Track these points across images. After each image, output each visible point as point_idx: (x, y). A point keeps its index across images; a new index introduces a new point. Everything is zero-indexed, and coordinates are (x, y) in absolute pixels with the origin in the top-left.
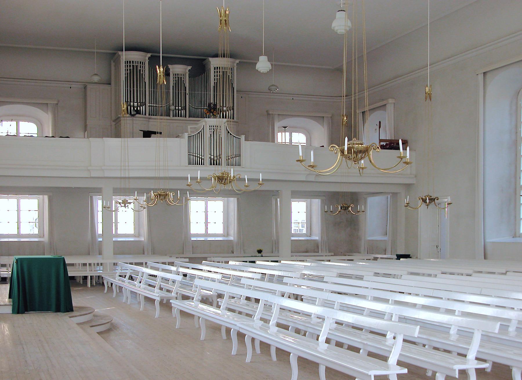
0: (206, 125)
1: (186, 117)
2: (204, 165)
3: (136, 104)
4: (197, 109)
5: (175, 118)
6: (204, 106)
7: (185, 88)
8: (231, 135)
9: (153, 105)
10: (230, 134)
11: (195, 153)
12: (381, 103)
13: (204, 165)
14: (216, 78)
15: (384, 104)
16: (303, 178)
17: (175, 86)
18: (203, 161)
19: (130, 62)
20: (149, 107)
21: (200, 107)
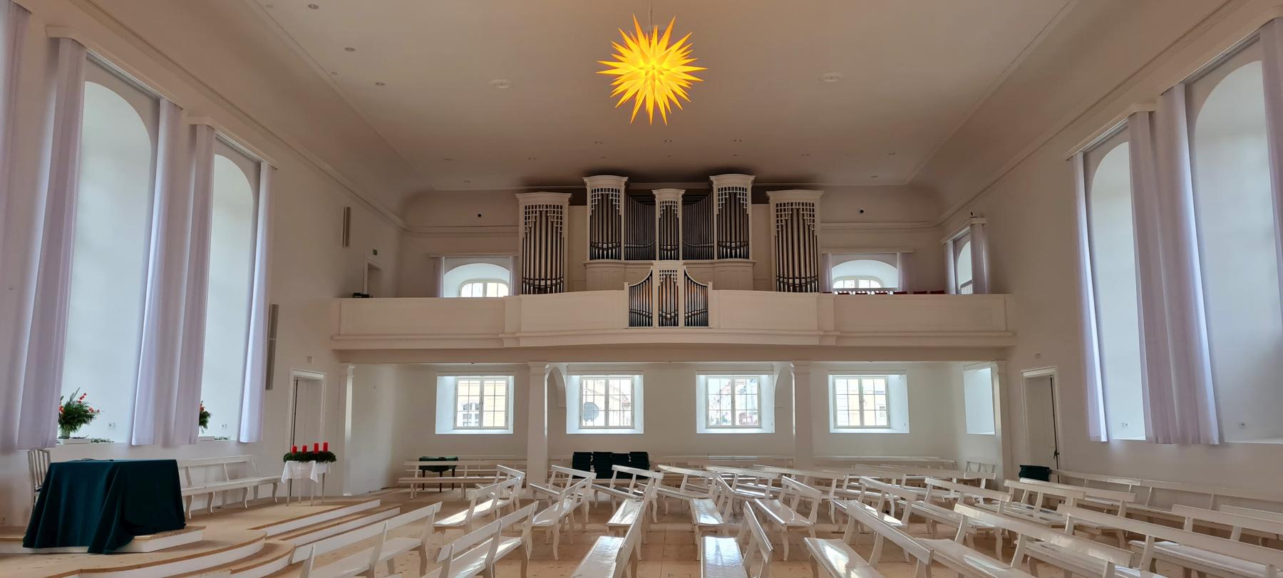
7: (678, 219)
8: (689, 281)
10: (692, 281)
19: (598, 190)
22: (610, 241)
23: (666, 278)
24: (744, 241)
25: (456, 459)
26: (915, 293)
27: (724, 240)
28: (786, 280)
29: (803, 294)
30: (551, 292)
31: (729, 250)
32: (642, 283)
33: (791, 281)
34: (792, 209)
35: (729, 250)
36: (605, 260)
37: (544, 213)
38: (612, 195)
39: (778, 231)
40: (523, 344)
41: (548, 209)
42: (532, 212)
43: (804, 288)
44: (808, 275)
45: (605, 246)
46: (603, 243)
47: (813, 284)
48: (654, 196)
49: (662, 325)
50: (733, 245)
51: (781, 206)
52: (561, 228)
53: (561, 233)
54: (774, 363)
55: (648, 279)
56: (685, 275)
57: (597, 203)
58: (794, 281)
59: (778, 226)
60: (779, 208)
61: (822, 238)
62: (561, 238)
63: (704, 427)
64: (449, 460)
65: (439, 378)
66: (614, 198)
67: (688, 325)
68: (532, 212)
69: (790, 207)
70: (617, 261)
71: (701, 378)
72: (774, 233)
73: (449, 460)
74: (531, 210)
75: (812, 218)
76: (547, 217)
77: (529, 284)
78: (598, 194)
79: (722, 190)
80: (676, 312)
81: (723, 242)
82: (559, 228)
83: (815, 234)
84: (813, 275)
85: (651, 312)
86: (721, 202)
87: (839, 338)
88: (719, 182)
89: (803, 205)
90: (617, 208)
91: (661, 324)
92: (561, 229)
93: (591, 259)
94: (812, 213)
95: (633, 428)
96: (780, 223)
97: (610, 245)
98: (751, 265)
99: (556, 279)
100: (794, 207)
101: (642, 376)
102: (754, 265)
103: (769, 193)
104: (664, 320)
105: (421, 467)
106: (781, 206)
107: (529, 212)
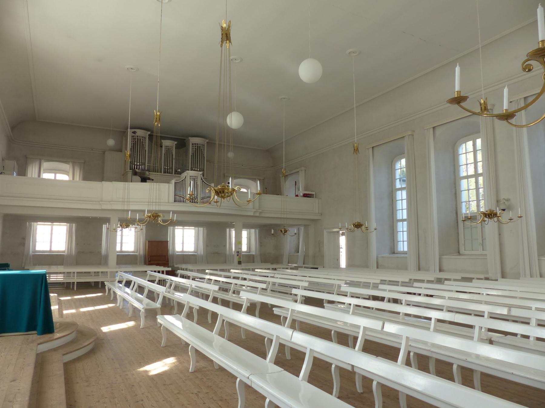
0: (187, 175)
1: (172, 174)
2: (185, 202)
3: (138, 164)
5: (165, 174)
7: (173, 155)
12: (297, 170)
13: (185, 202)
14: (193, 150)
15: (298, 171)
16: (252, 214)
24: (201, 169)
46: (137, 162)
56: (202, 179)
87: (260, 213)
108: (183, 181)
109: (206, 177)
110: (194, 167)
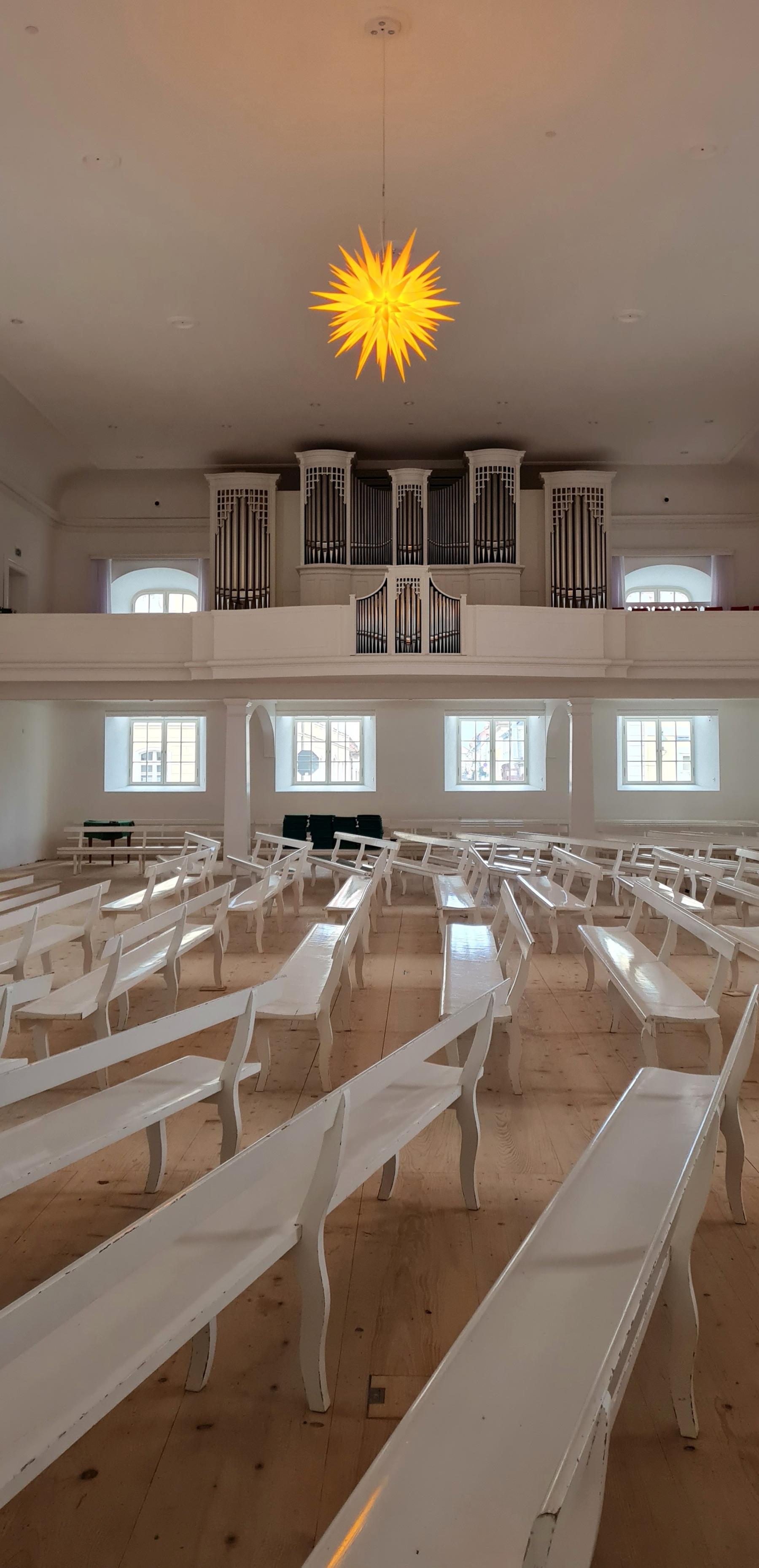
4: (445, 547)
6: (457, 541)
7: (422, 509)
9: (359, 545)
10: (439, 593)
11: (369, 630)
17: (401, 508)
18: (384, 645)
20: (353, 550)
21: (492, 541)
22: (331, 538)
23: (405, 589)
24: (509, 540)
25: (131, 824)
26: (733, 609)
27: (483, 538)
28: (563, 592)
29: (587, 610)
30: (254, 607)
31: (489, 552)
32: (374, 595)
33: (570, 593)
34: (574, 496)
35: (489, 552)
36: (325, 565)
37: (243, 502)
38: (334, 476)
39: (555, 527)
40: (218, 674)
41: (249, 496)
42: (228, 498)
43: (587, 602)
44: (593, 585)
45: (325, 545)
46: (322, 542)
47: (600, 597)
48: (390, 479)
49: (400, 651)
50: (495, 544)
51: (559, 492)
52: (266, 521)
53: (266, 528)
54: (547, 701)
55: (382, 590)
56: (431, 584)
57: (313, 487)
58: (574, 593)
59: (555, 519)
60: (557, 495)
61: (613, 535)
62: (266, 534)
63: (455, 782)
64: (123, 825)
65: (107, 719)
66: (337, 481)
67: (434, 651)
68: (228, 498)
69: (571, 494)
70: (340, 565)
71: (452, 721)
72: (549, 529)
73: (123, 825)
74: (225, 496)
75: (600, 509)
76: (247, 506)
77: (225, 596)
78: (315, 476)
79: (481, 471)
80: (418, 634)
81: (481, 540)
82: (263, 522)
83: (603, 531)
84: (599, 585)
85: (385, 634)
86: (479, 487)
87: (631, 668)
88: (478, 459)
89: (588, 492)
90: (341, 495)
91: (399, 650)
92: (266, 523)
93: (306, 563)
94: (600, 502)
95: (363, 784)
96: (557, 516)
97: (331, 544)
98: (519, 572)
99: (260, 589)
100: (576, 494)
101: (374, 717)
102: (522, 572)
103: (544, 475)
104: (402, 645)
105: (86, 834)
106: (559, 492)
107: (223, 498)
108: (380, 593)
109: (521, 564)
110: (489, 538)
